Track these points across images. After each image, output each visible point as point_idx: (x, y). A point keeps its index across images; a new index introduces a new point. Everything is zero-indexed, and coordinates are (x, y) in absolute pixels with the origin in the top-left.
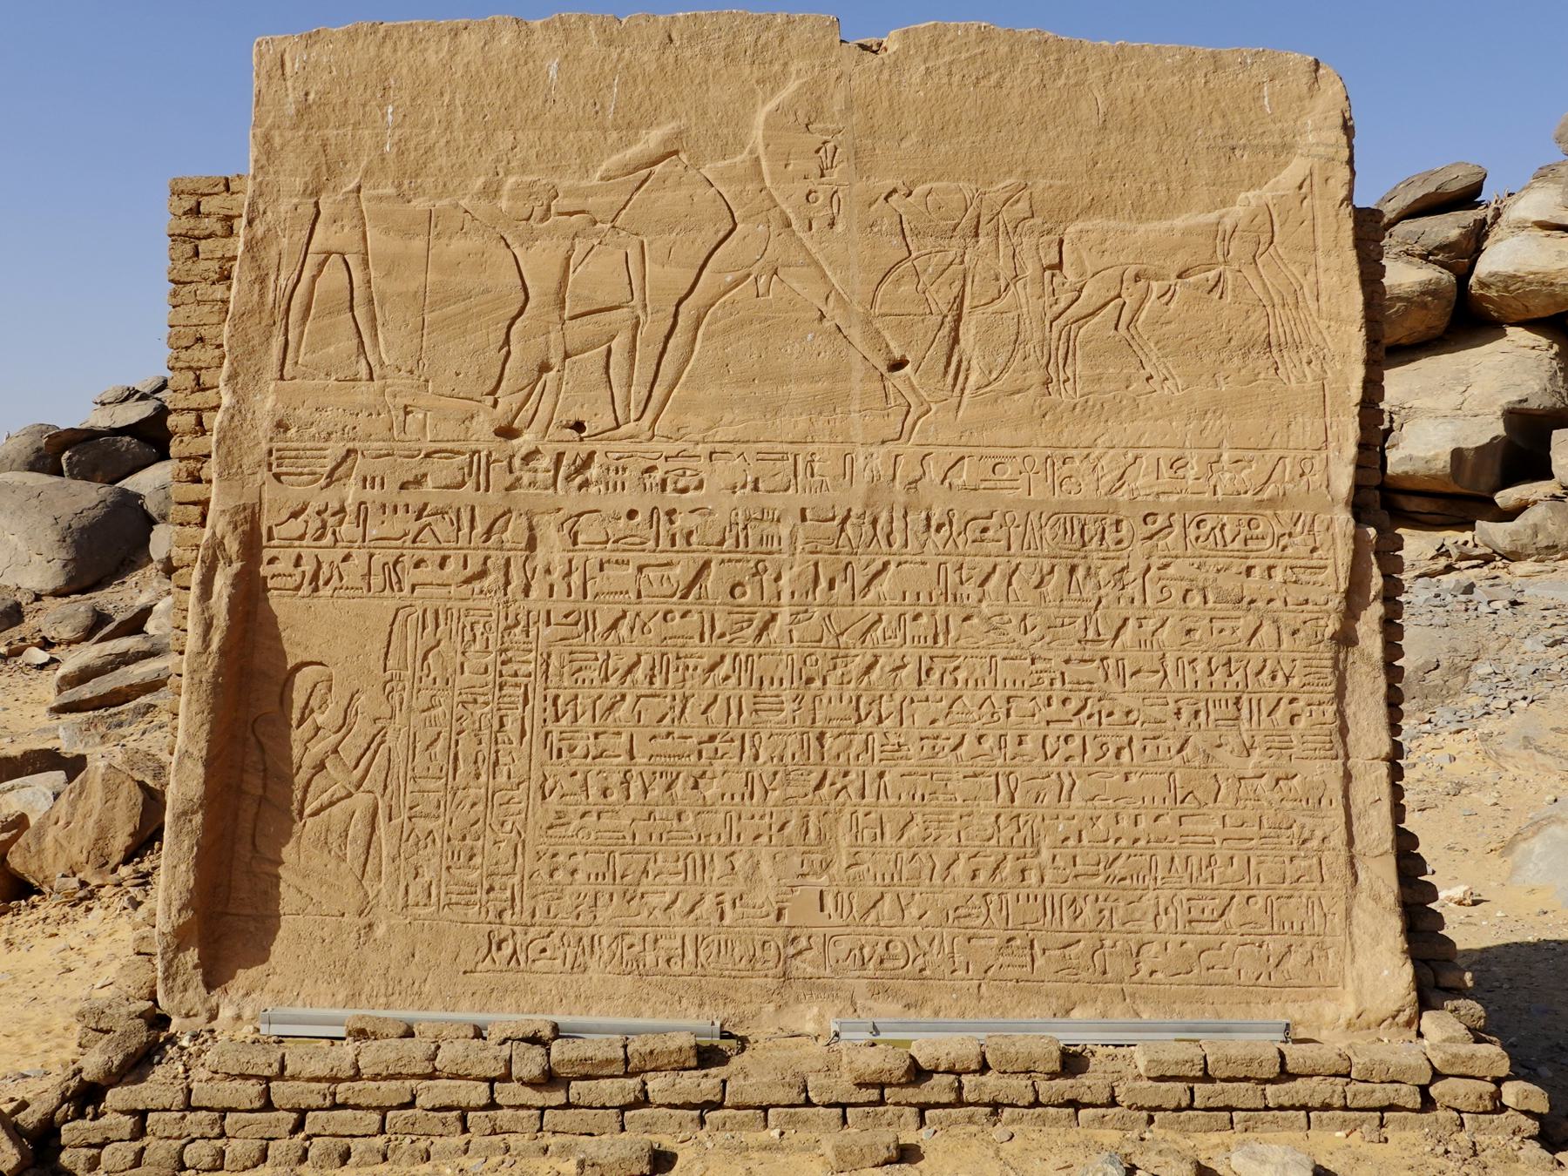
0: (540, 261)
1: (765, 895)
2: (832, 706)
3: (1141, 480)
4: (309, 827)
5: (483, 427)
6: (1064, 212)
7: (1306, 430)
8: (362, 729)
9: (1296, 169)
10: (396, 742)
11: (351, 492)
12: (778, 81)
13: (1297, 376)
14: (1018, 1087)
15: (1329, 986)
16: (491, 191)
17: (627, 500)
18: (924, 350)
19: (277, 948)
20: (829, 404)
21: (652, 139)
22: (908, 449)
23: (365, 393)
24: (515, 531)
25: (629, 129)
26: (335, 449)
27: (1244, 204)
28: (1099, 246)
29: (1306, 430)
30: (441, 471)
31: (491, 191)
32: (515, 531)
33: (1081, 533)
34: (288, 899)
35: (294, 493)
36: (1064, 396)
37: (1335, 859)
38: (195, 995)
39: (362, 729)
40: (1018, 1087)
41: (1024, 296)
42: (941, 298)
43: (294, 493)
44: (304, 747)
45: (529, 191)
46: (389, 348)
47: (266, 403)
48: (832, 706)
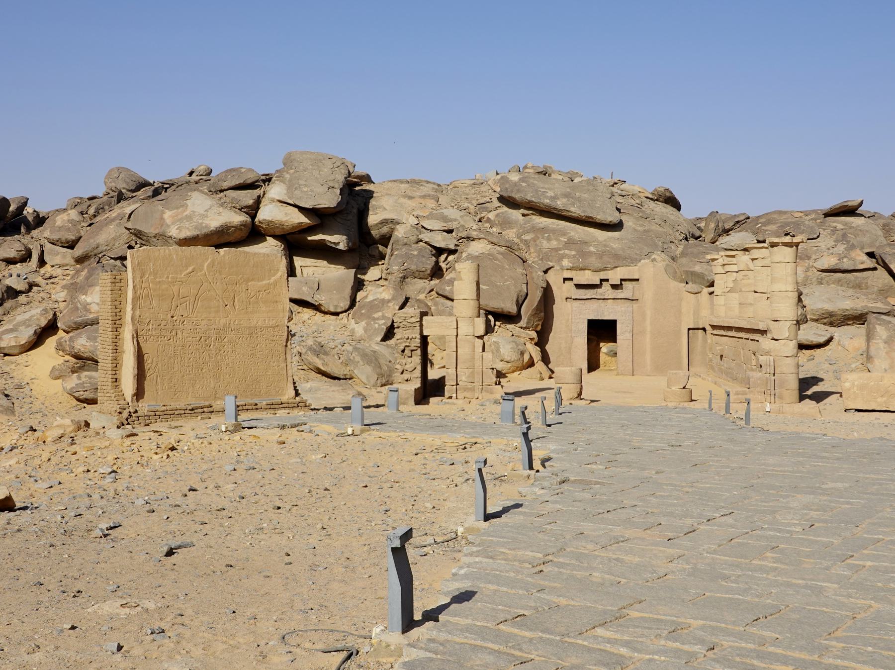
0: (175, 289)
1: (212, 386)
2: (219, 358)
3: (260, 323)
4: (148, 378)
5: (169, 316)
6: (248, 280)
7: (281, 315)
8: (154, 363)
9: (279, 274)
10: (160, 365)
11: (151, 326)
12: (207, 259)
13: (280, 307)
14: (250, 407)
15: (284, 395)
16: (168, 277)
17: (190, 327)
18: (230, 304)
19: (145, 396)
20: (217, 312)
21: (190, 269)
22: (228, 318)
23: (152, 311)
24: (174, 332)
25: (187, 267)
26: (148, 320)
27: (273, 279)
28: (254, 285)
29: (281, 315)
30: (163, 323)
31: (168, 277)
32: (174, 332)
33: (252, 331)
34: (146, 390)
35: (143, 327)
36: (249, 310)
37: (285, 377)
38: (136, 403)
39: (154, 363)
40: (250, 407)
41: (243, 294)
42: (232, 295)
43: (143, 327)
44: (147, 367)
45: (172, 278)
46: (154, 304)
47: (138, 313)
48: (219, 358)
